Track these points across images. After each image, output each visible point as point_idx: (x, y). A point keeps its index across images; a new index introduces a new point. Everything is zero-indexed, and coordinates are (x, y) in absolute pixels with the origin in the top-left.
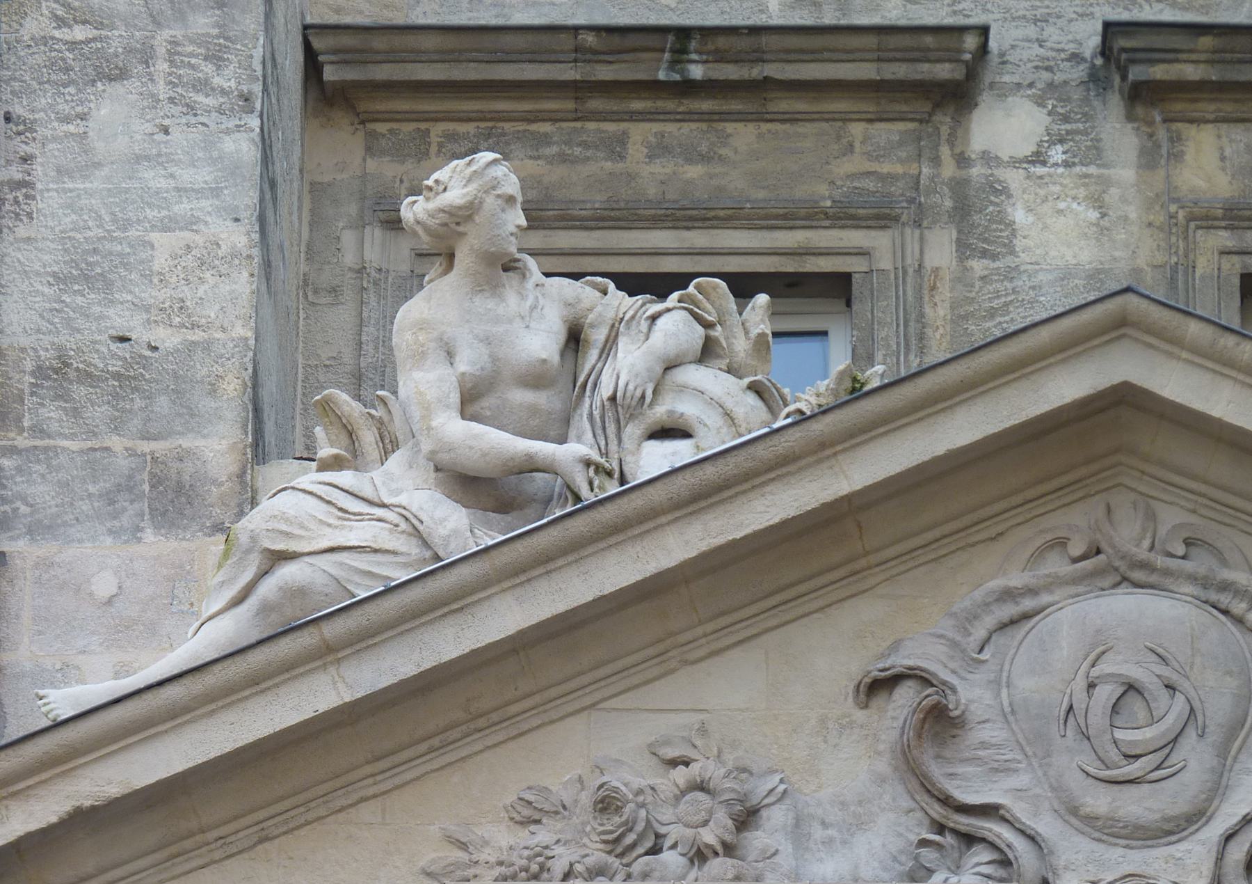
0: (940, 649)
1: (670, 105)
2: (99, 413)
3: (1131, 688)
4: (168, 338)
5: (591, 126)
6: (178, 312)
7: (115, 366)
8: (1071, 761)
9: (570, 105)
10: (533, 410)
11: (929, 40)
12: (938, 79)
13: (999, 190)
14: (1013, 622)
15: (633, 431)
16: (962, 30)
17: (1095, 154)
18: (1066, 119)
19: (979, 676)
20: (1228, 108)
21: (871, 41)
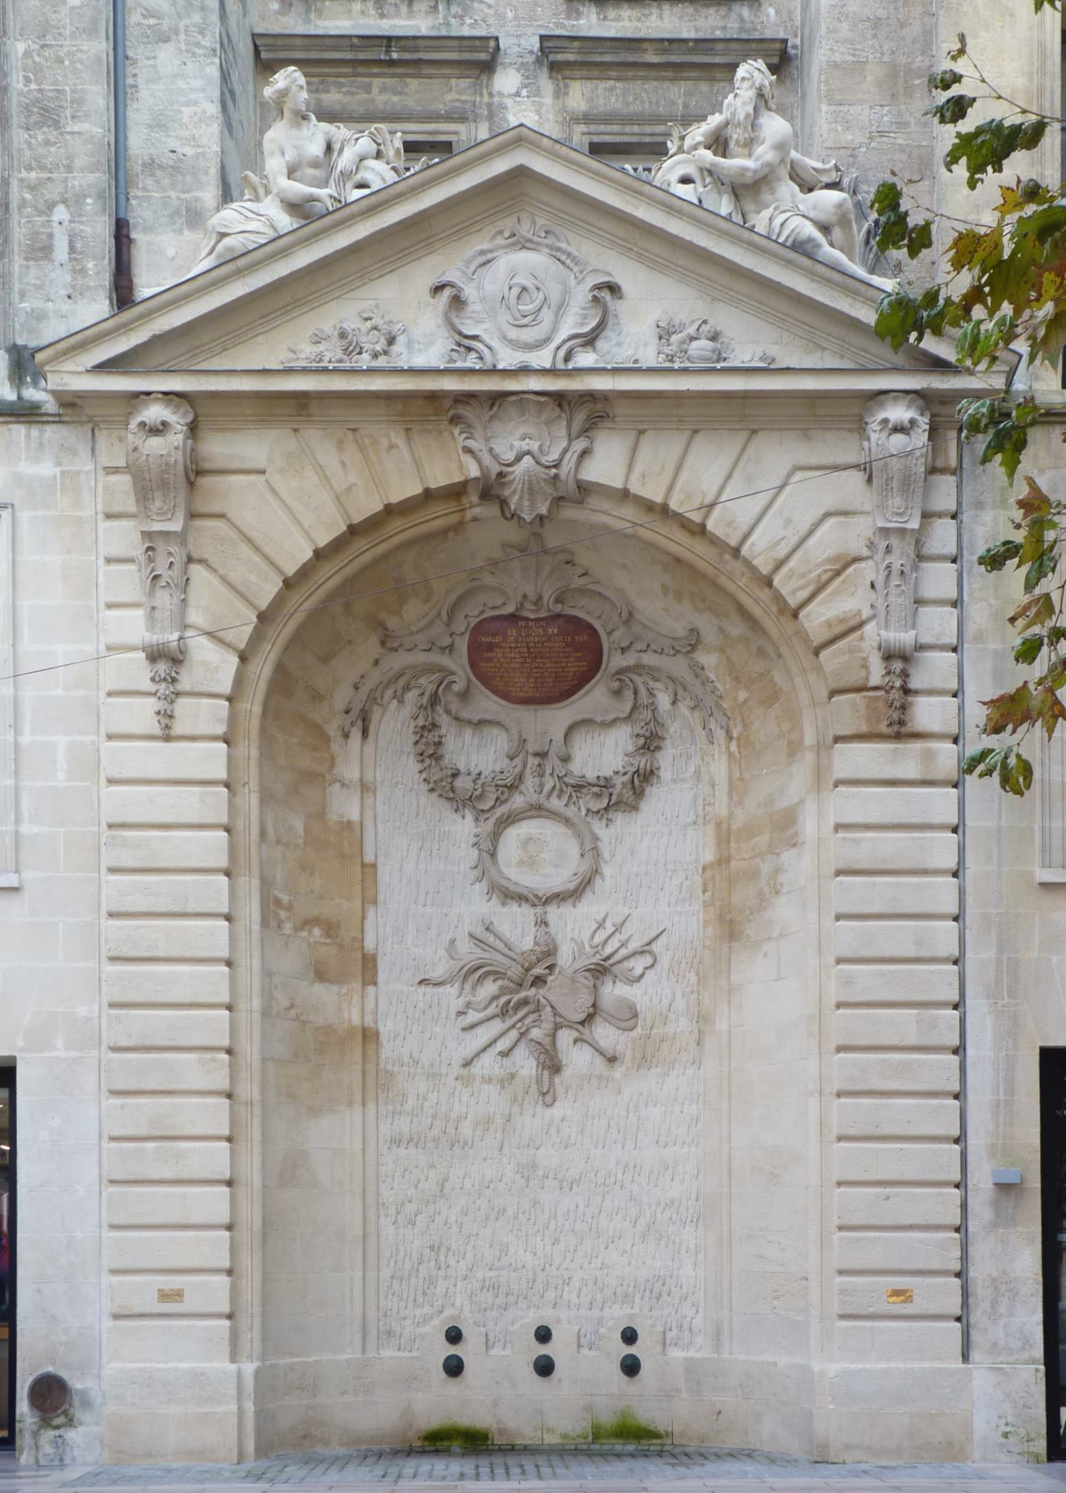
0: (458, 274)
1: (386, 70)
2: (166, 182)
3: (524, 289)
4: (189, 151)
5: (359, 79)
6: (192, 140)
7: (171, 163)
8: (504, 318)
9: (350, 70)
10: (315, 178)
11: (477, 43)
12: (481, 59)
13: (503, 107)
14: (485, 264)
15: (349, 185)
16: (487, 38)
17: (537, 93)
18: (528, 78)
19: (472, 285)
20: (585, 73)
21: (456, 43)
